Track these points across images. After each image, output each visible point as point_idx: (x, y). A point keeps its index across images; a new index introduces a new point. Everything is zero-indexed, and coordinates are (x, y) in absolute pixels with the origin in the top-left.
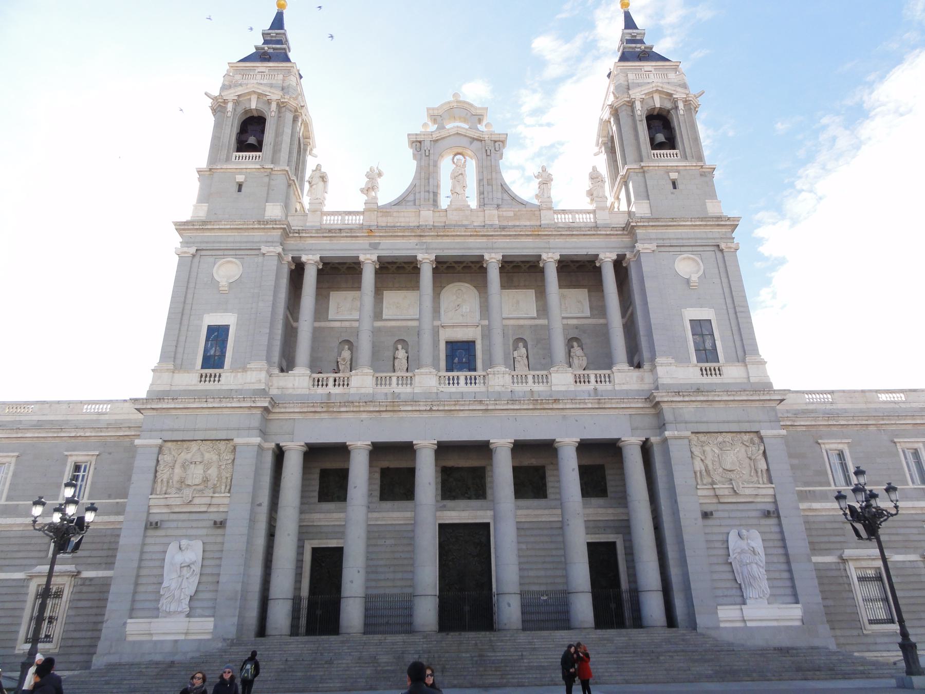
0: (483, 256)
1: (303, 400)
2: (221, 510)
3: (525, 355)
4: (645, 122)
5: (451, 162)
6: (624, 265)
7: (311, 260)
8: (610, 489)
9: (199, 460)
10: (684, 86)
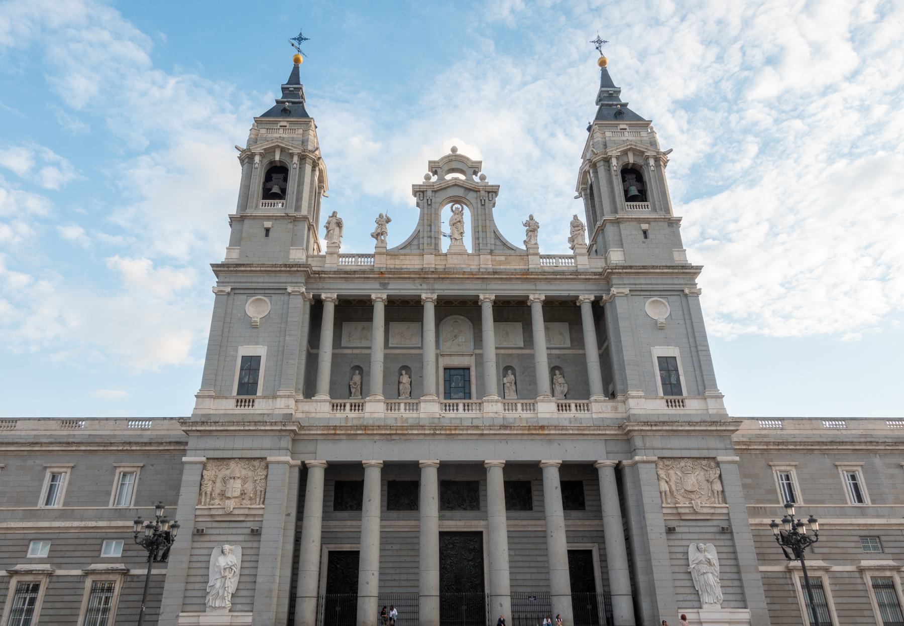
0: (479, 296)
2: (256, 519)
3: (514, 381)
4: (620, 177)
5: (450, 209)
6: (601, 305)
7: (329, 296)
8: (587, 503)
9: (238, 475)
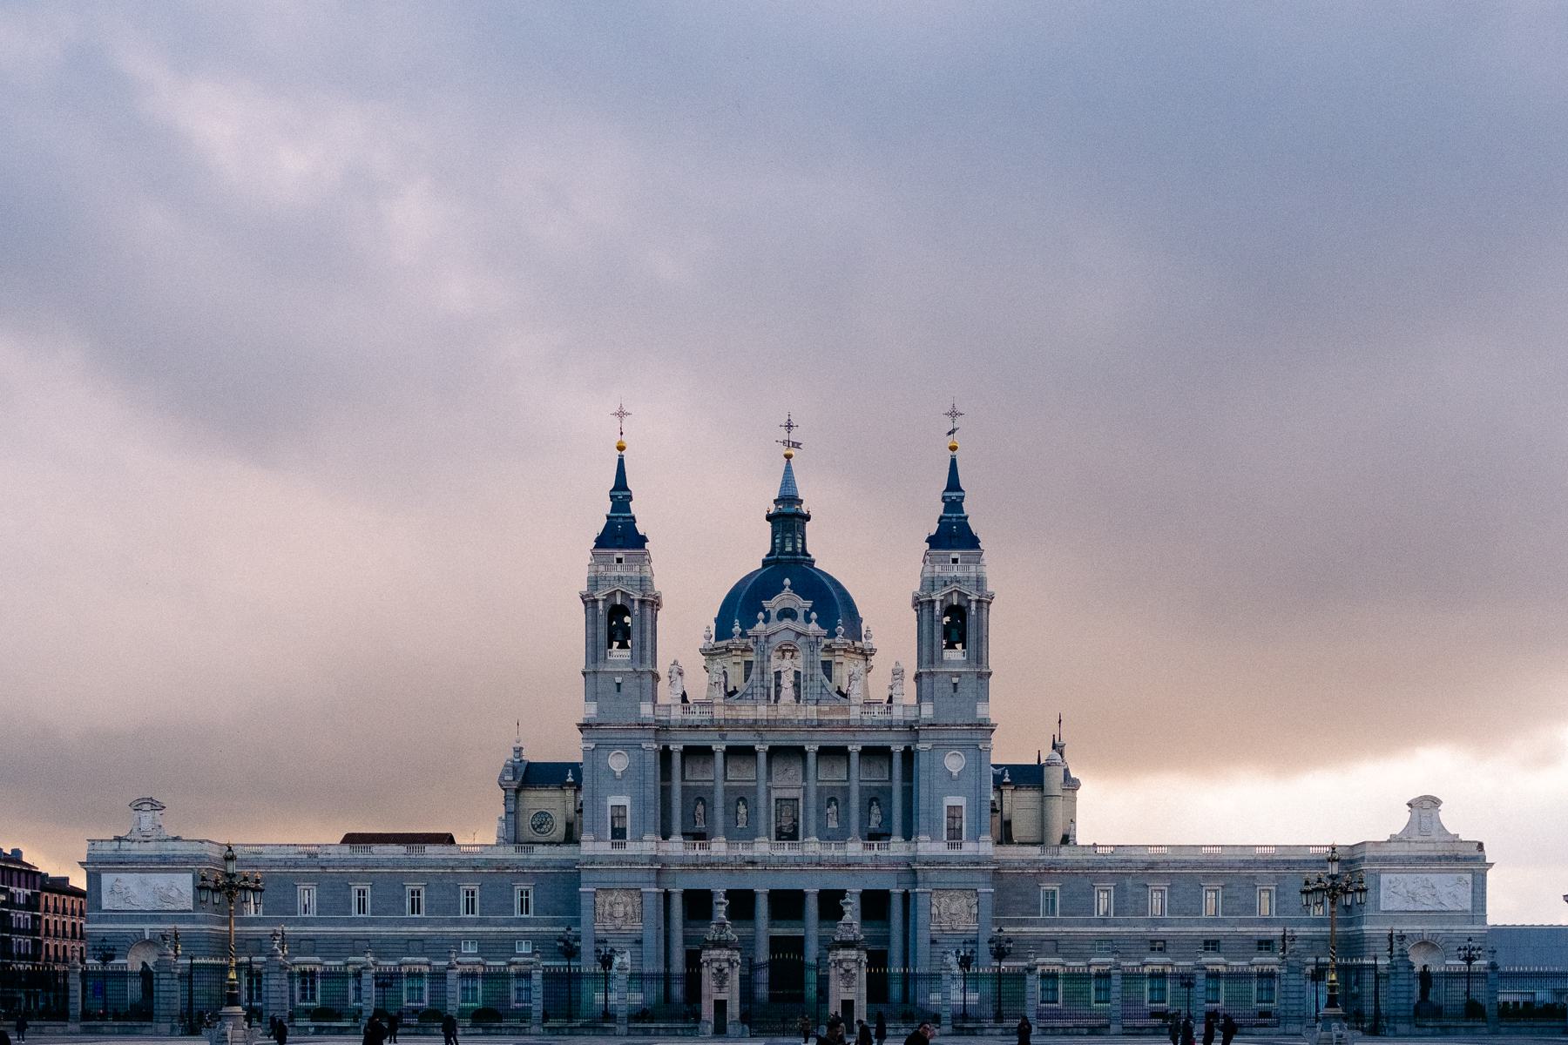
7: (676, 747)
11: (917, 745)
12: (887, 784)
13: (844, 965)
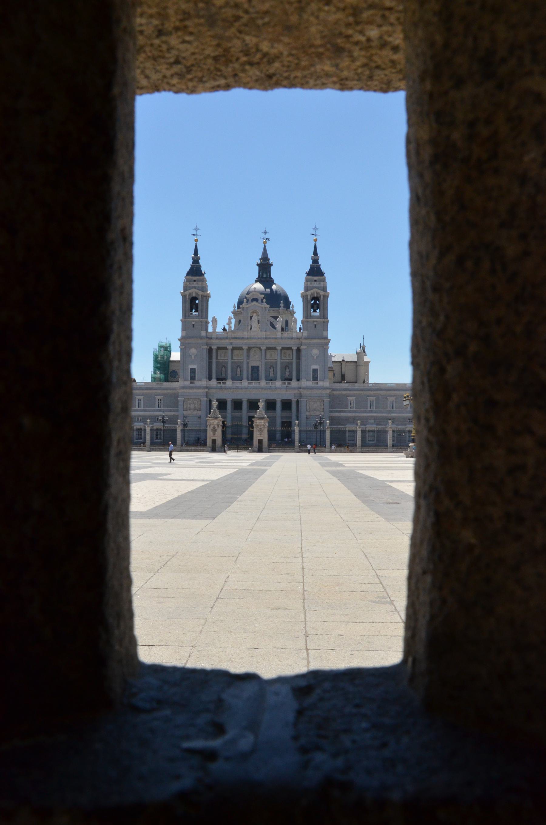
1: (216, 388)
10: (324, 289)
11: (302, 346)
12: (291, 361)
13: (259, 426)
